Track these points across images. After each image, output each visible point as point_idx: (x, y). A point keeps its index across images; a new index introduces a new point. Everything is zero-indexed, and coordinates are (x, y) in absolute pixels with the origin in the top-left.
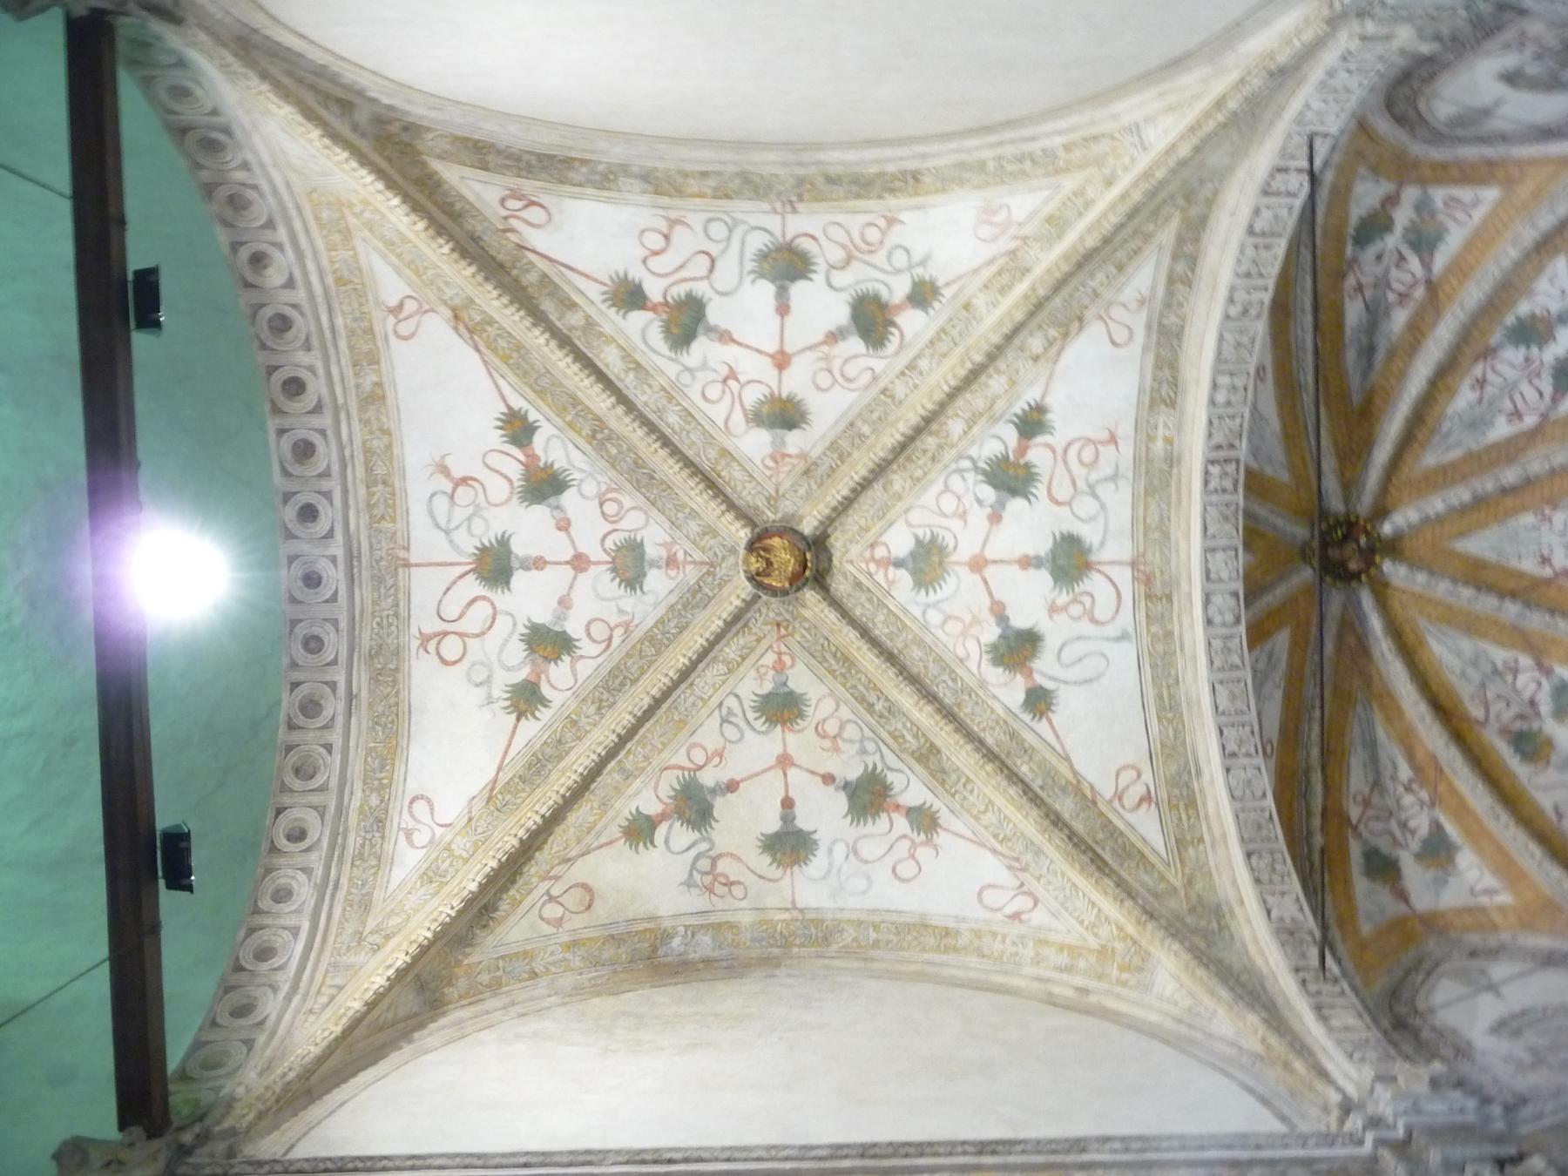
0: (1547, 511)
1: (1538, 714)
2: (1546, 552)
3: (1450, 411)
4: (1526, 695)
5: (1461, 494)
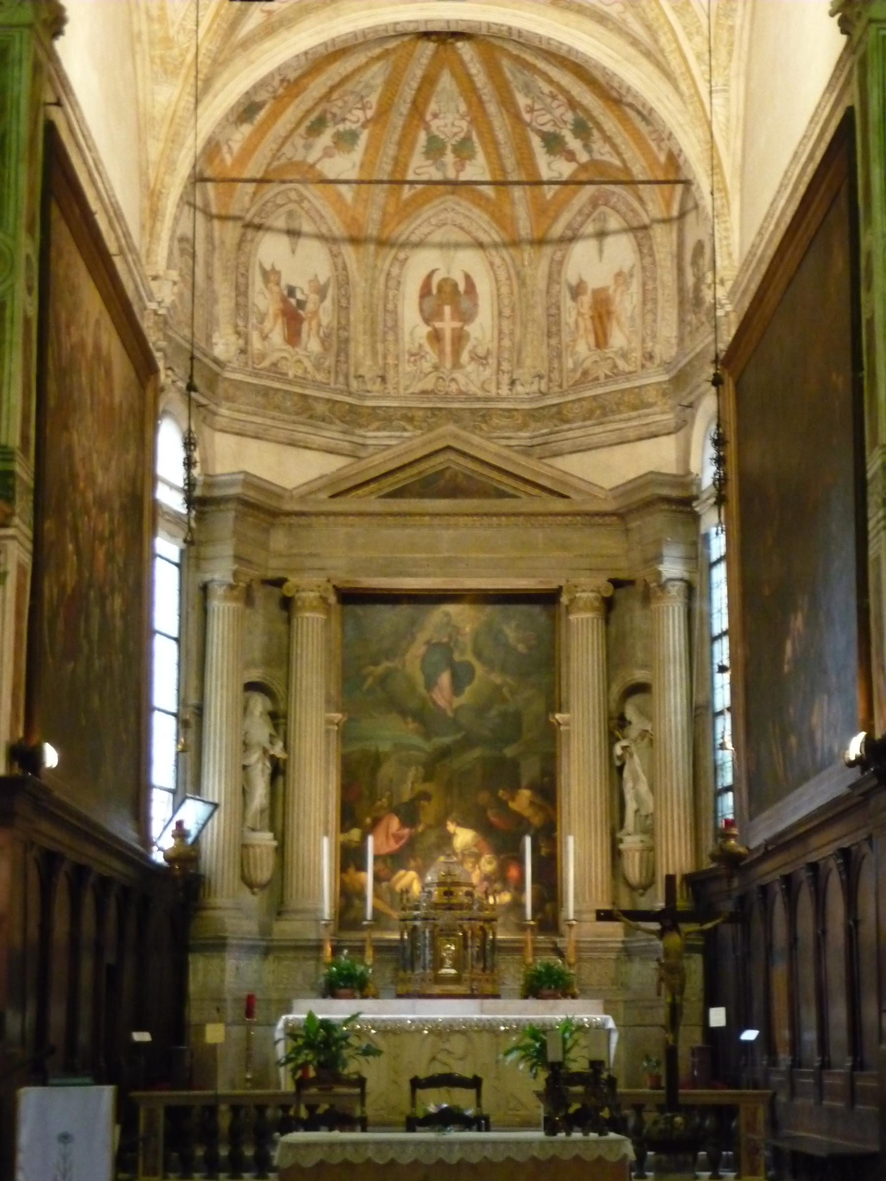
0: (468, 118)
1: (336, 124)
2: (442, 115)
3: (536, 76)
4: (349, 116)
5: (480, 79)
